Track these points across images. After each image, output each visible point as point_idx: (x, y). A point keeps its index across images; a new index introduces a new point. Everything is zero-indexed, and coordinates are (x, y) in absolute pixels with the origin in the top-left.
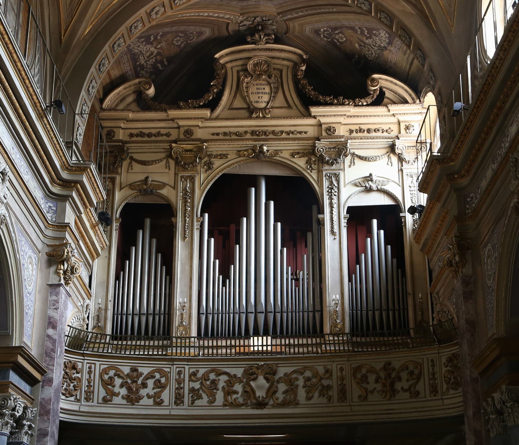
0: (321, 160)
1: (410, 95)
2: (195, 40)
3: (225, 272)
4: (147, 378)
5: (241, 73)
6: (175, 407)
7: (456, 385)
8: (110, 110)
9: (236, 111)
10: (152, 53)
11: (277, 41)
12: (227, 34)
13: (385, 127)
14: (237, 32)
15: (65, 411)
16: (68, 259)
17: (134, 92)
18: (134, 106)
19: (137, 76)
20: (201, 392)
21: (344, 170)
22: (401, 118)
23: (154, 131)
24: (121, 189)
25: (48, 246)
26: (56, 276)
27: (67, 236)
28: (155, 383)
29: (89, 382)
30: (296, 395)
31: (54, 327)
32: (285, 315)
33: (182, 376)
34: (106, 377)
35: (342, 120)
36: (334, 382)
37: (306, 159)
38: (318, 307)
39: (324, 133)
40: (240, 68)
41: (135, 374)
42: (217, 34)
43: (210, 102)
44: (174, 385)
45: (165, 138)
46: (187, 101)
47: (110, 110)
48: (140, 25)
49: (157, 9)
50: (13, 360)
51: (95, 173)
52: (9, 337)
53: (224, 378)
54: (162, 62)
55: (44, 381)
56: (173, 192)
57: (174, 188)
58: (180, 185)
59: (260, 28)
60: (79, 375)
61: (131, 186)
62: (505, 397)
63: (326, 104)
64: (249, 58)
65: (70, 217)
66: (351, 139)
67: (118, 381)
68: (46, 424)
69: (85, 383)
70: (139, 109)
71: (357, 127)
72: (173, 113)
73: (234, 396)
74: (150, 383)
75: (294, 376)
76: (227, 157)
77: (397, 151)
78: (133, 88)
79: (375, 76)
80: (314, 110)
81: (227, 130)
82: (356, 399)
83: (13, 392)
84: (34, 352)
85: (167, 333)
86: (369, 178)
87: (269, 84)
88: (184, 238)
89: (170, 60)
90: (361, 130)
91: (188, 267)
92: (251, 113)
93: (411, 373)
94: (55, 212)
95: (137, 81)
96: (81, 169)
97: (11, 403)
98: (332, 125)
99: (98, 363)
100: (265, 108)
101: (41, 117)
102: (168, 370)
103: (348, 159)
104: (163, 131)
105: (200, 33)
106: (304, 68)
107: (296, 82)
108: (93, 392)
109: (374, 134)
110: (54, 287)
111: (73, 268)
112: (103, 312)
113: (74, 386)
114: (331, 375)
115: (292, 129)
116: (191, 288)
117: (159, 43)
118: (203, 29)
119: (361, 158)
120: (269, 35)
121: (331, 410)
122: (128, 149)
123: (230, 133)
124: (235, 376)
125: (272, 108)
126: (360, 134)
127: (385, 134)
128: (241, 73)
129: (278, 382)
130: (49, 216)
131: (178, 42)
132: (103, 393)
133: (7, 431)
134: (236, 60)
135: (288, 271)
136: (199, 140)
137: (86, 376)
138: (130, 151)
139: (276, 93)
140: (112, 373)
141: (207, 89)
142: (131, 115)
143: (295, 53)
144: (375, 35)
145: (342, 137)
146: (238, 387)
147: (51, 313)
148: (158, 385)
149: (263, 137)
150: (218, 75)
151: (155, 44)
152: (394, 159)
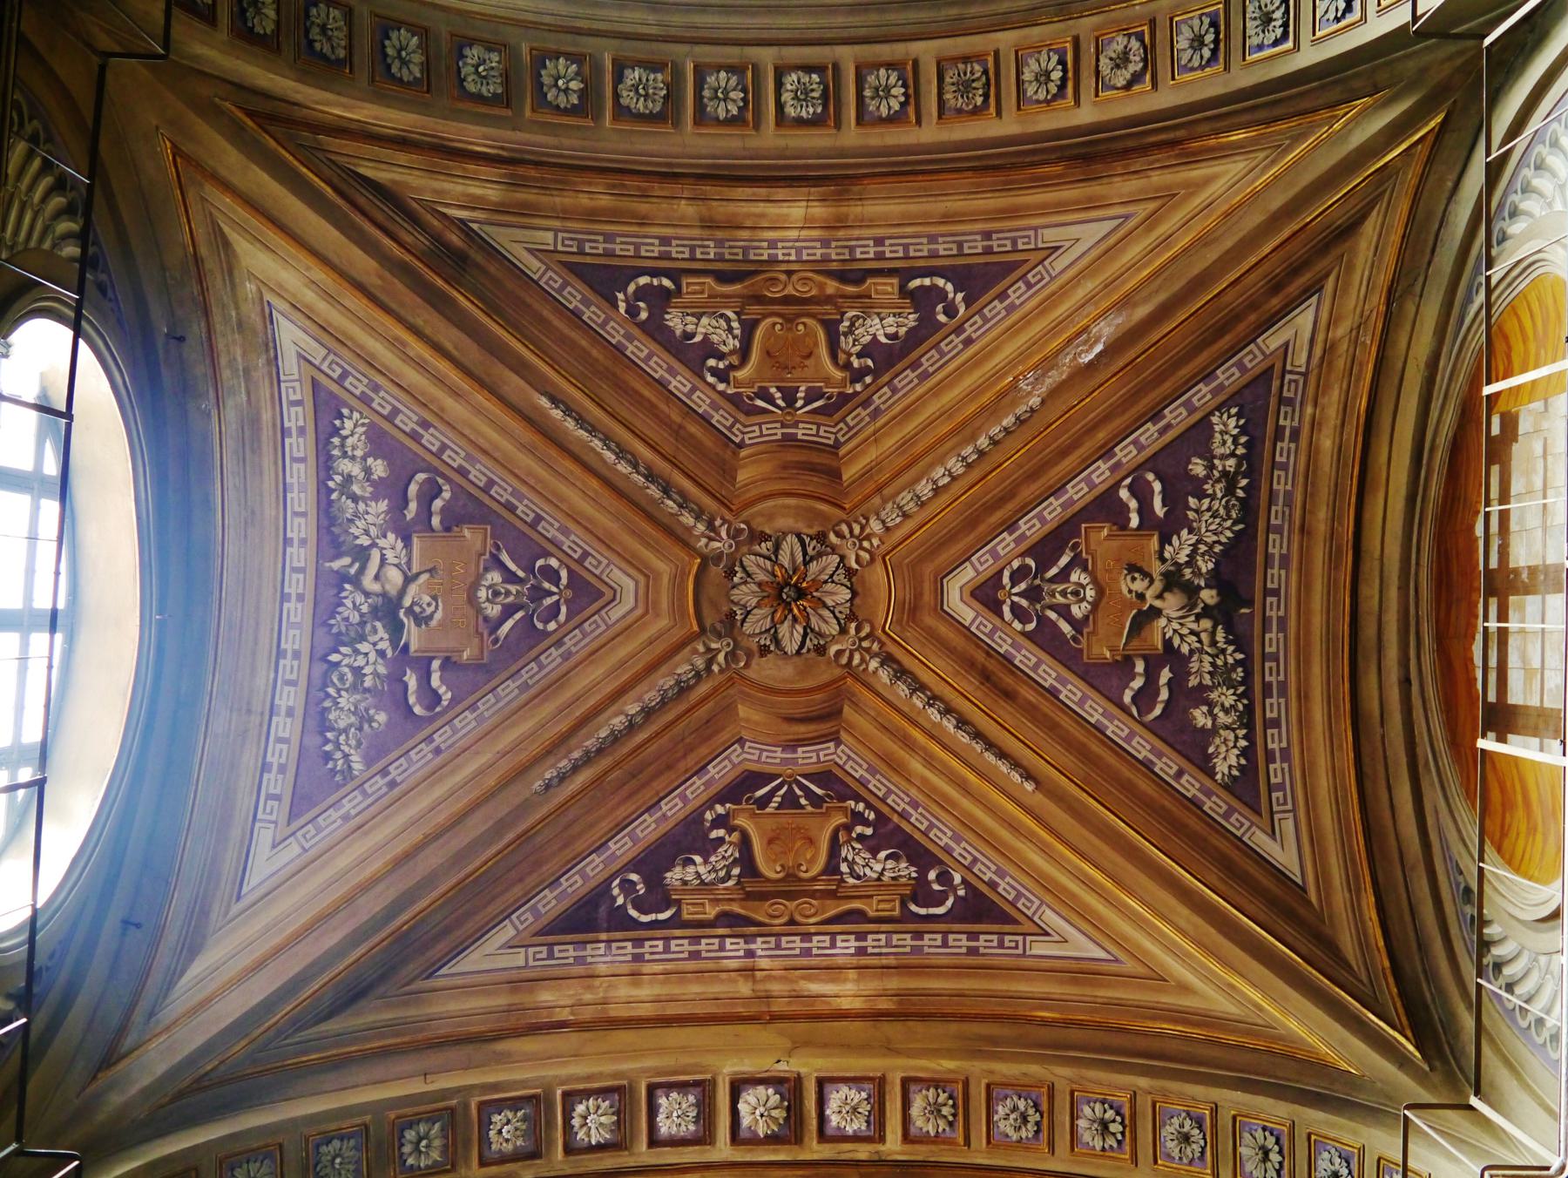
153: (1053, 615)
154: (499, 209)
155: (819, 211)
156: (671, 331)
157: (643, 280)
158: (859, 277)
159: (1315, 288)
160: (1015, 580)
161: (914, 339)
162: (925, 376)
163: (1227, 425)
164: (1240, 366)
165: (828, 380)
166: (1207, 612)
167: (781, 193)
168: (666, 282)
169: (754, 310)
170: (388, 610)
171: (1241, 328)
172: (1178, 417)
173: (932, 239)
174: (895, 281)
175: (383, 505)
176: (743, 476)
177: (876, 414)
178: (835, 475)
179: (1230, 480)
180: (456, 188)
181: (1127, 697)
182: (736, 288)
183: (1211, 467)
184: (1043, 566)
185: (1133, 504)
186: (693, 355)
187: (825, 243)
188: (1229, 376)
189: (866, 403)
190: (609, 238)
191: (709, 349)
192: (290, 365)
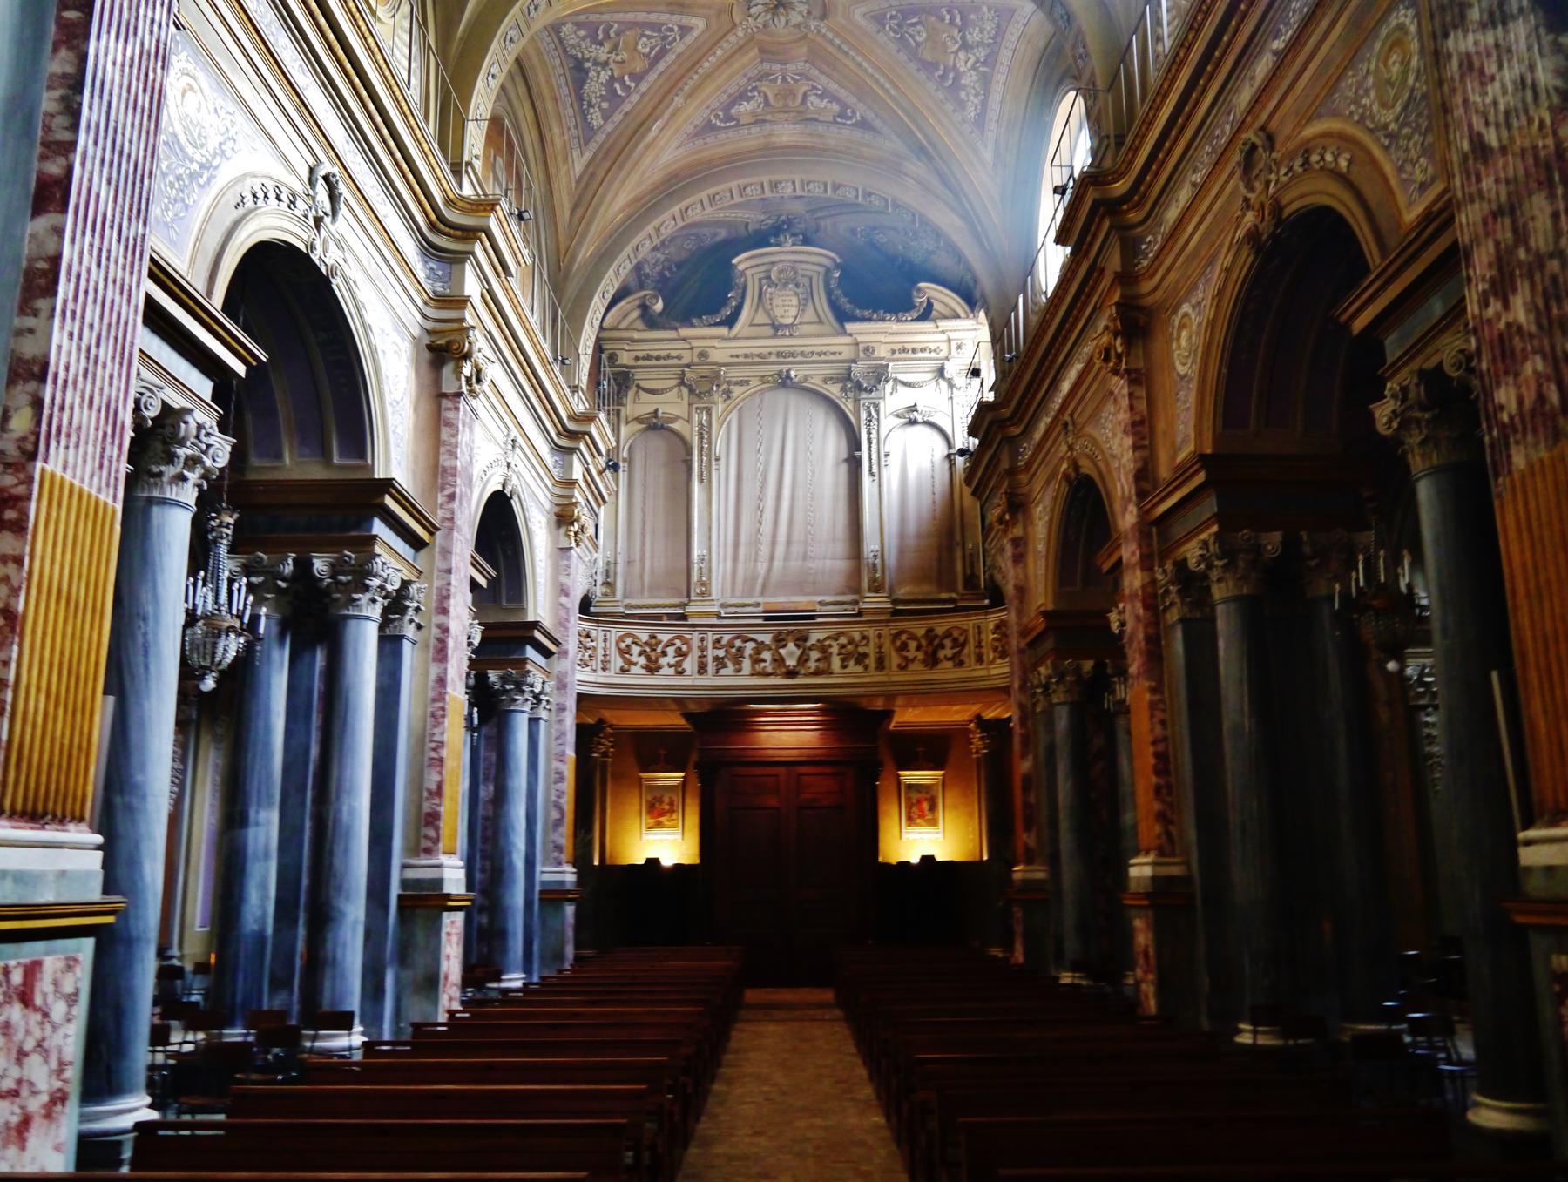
0: (858, 387)
2: (708, 242)
5: (764, 281)
7: (1003, 655)
8: (611, 329)
10: (658, 260)
11: (806, 242)
13: (933, 346)
14: (757, 232)
15: (582, 683)
16: (578, 520)
17: (639, 307)
18: (640, 324)
19: (642, 288)
21: (884, 398)
22: (952, 335)
23: (663, 353)
24: (627, 423)
28: (676, 651)
30: (829, 665)
31: (567, 595)
34: (623, 645)
35: (882, 338)
36: (871, 650)
39: (862, 355)
40: (762, 275)
41: (654, 641)
43: (727, 317)
44: (696, 653)
46: (700, 317)
47: (611, 329)
48: (648, 242)
51: (604, 421)
52: (523, 610)
53: (750, 646)
56: (688, 426)
58: (696, 418)
60: (594, 644)
61: (638, 420)
62: (1050, 671)
64: (773, 263)
65: (578, 473)
66: (893, 360)
67: (636, 650)
69: (600, 652)
71: (900, 346)
72: (684, 332)
73: (763, 665)
75: (827, 643)
77: (947, 375)
78: (637, 303)
79: (922, 285)
80: (850, 327)
81: (747, 351)
82: (894, 667)
84: (547, 623)
86: (913, 408)
87: (797, 294)
88: (701, 481)
89: (679, 266)
90: (905, 350)
91: (706, 514)
93: (955, 640)
94: (562, 467)
96: (589, 419)
97: (529, 680)
100: (792, 325)
103: (889, 386)
104: (674, 353)
105: (715, 235)
106: (837, 275)
107: (829, 293)
109: (920, 355)
112: (612, 566)
115: (824, 349)
117: (668, 247)
119: (905, 384)
121: (868, 680)
123: (753, 355)
127: (933, 355)
128: (764, 281)
129: (810, 649)
130: (555, 472)
131: (689, 245)
132: (620, 662)
137: (601, 645)
139: (805, 305)
140: (629, 640)
141: (724, 301)
142: (636, 335)
146: (767, 655)
147: (563, 579)
148: (681, 654)
152: (943, 384)
155: (774, 139)
158: (756, 122)
159: (578, 181)
160: (675, 39)
162: (725, 92)
163: (596, 118)
169: (802, 109)
170: (965, 46)
171: (600, 156)
172: (618, 117)
175: (963, 81)
176: (804, 50)
177: (745, 75)
178: (762, 51)
179: (590, 105)
182: (809, 116)
185: (628, 83)
188: (600, 138)
189: (750, 79)
191: (821, 97)
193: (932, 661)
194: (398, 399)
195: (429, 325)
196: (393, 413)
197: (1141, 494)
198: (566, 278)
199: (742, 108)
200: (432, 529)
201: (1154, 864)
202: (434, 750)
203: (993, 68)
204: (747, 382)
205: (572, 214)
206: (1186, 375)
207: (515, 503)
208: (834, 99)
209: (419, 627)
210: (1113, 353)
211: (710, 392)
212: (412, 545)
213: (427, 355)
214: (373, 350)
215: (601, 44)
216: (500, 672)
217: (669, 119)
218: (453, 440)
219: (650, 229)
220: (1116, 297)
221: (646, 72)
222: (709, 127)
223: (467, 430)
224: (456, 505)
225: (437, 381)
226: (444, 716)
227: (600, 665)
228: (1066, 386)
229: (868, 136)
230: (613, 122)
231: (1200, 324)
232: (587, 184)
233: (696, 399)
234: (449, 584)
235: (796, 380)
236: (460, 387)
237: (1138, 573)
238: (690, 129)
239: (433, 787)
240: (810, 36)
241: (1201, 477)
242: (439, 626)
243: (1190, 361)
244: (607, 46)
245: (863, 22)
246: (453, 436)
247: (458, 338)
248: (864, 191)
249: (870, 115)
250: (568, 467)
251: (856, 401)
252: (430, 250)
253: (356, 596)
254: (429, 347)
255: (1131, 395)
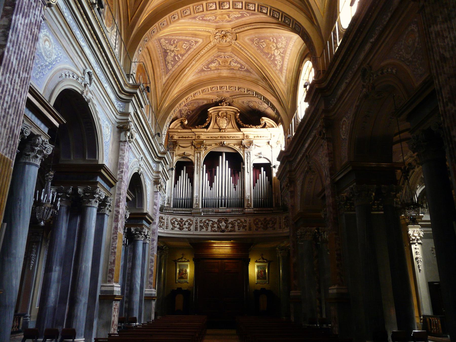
0: (244, 147)
1: (275, 125)
2: (201, 104)
3: (211, 185)
4: (186, 222)
6: (195, 231)
7: (287, 226)
8: (172, 129)
9: (215, 129)
10: (186, 109)
11: (230, 105)
12: (212, 102)
14: (216, 102)
15: (160, 232)
16: (160, 183)
17: (180, 122)
18: (180, 128)
19: (181, 117)
20: (203, 227)
21: (252, 150)
23: (187, 136)
24: (176, 156)
25: (154, 178)
26: (156, 189)
27: (160, 175)
28: (188, 224)
29: (167, 223)
30: (235, 228)
31: (156, 206)
32: (231, 200)
33: (197, 221)
34: (172, 221)
36: (247, 224)
37: (239, 146)
38: (242, 198)
39: (245, 137)
40: (216, 114)
41: (182, 220)
42: (209, 102)
43: (206, 126)
44: (194, 224)
45: (191, 139)
46: (198, 126)
47: (172, 129)
48: (184, 103)
49: (189, 98)
50: (144, 217)
52: (143, 209)
53: (211, 222)
54: (190, 112)
55: (153, 223)
57: (194, 156)
58: (196, 155)
59: (224, 101)
60: (164, 221)
61: (179, 155)
63: (246, 127)
64: (220, 111)
67: (176, 223)
68: (154, 237)
69: (166, 223)
70: (182, 129)
72: (193, 130)
73: (214, 228)
74: (187, 223)
75: (234, 222)
76: (212, 146)
78: (180, 121)
79: (263, 118)
80: (242, 129)
81: (212, 136)
82: (254, 230)
83: (144, 227)
84: (150, 214)
85: (191, 206)
86: (260, 153)
87: (227, 120)
88: (197, 174)
89: (193, 111)
91: (198, 183)
92: (220, 130)
94: (156, 167)
95: (181, 119)
96: (164, 153)
97: (144, 231)
98: (248, 135)
99: (170, 217)
100: (225, 129)
101: (153, 138)
102: (193, 219)
104: (190, 136)
105: (203, 102)
106: (238, 114)
107: (236, 119)
108: (168, 226)
110: (156, 192)
111: (162, 185)
112: (170, 198)
113: (162, 224)
114: (247, 222)
115: (234, 136)
116: (199, 191)
118: (204, 101)
120: (226, 103)
122: (178, 142)
124: (215, 222)
125: (228, 128)
126: (257, 138)
127: (266, 138)
128: (217, 116)
129: (229, 224)
130: (154, 169)
132: (171, 227)
133: (143, 240)
134: (215, 111)
135: (232, 185)
136: (202, 139)
137: (166, 221)
138: (179, 143)
139: (229, 123)
140: (174, 220)
141: (205, 122)
142: (179, 131)
143: (236, 109)
144: (263, 104)
145: (252, 139)
146: (216, 225)
147: (155, 201)
148: (189, 224)
149: (224, 138)
150: (209, 117)
151: (187, 106)
153: (188, 43)
154: (259, 81)
155: (222, 74)
156: (240, 64)
157: (243, 70)
158: (216, 69)
159: (164, 84)
160: (193, 45)
161: (209, 64)
162: (207, 60)
163: (170, 67)
164: (170, 74)
165: (220, 59)
166: (168, 50)
167: (226, 76)
168: (240, 69)
169: (229, 66)
170: (277, 48)
171: (171, 77)
172: (176, 67)
173: (208, 74)
174: (212, 69)
176: (231, 49)
177: (213, 56)
178: (218, 49)
179: (168, 63)
180: (263, 84)
181: (176, 40)
183: (171, 63)
184: (190, 47)
186: (236, 62)
187: (221, 72)
188: (171, 72)
189: (215, 57)
190: (247, 74)
191: (235, 62)
192: (284, 77)
193: (265, 228)
194: (107, 141)
195: (118, 121)
196: (105, 145)
197: (331, 174)
198: (159, 112)
199: (212, 65)
200: (115, 181)
201: (337, 289)
202: (113, 249)
203: (285, 55)
204: (211, 145)
205: (162, 93)
206: (345, 138)
207: (141, 177)
208: (239, 63)
209: (110, 211)
210: (322, 133)
211: (200, 148)
212: (109, 186)
213: (117, 129)
214: (100, 126)
215: (172, 45)
216: (135, 228)
217: (191, 68)
218: (123, 155)
219: (184, 99)
220: (323, 116)
221: (185, 54)
222: (202, 71)
223: (127, 152)
224: (123, 174)
225: (119, 137)
226: (117, 239)
227: (165, 227)
228: (307, 145)
229: (249, 74)
230: (175, 68)
231: (349, 123)
232: (167, 86)
233: (196, 149)
234: (120, 198)
235: (226, 145)
236: (126, 139)
237: (331, 198)
238: (197, 71)
239: (112, 261)
240: (232, 45)
241: (350, 169)
242: (116, 211)
243: (346, 134)
244: (174, 46)
245: (248, 41)
246: (123, 153)
247: (126, 125)
248: (247, 90)
249: (249, 68)
250: (158, 167)
251: (244, 151)
252: (119, 99)
253: (91, 200)
254: (118, 127)
255: (328, 145)
